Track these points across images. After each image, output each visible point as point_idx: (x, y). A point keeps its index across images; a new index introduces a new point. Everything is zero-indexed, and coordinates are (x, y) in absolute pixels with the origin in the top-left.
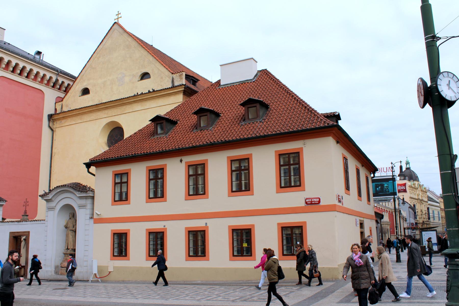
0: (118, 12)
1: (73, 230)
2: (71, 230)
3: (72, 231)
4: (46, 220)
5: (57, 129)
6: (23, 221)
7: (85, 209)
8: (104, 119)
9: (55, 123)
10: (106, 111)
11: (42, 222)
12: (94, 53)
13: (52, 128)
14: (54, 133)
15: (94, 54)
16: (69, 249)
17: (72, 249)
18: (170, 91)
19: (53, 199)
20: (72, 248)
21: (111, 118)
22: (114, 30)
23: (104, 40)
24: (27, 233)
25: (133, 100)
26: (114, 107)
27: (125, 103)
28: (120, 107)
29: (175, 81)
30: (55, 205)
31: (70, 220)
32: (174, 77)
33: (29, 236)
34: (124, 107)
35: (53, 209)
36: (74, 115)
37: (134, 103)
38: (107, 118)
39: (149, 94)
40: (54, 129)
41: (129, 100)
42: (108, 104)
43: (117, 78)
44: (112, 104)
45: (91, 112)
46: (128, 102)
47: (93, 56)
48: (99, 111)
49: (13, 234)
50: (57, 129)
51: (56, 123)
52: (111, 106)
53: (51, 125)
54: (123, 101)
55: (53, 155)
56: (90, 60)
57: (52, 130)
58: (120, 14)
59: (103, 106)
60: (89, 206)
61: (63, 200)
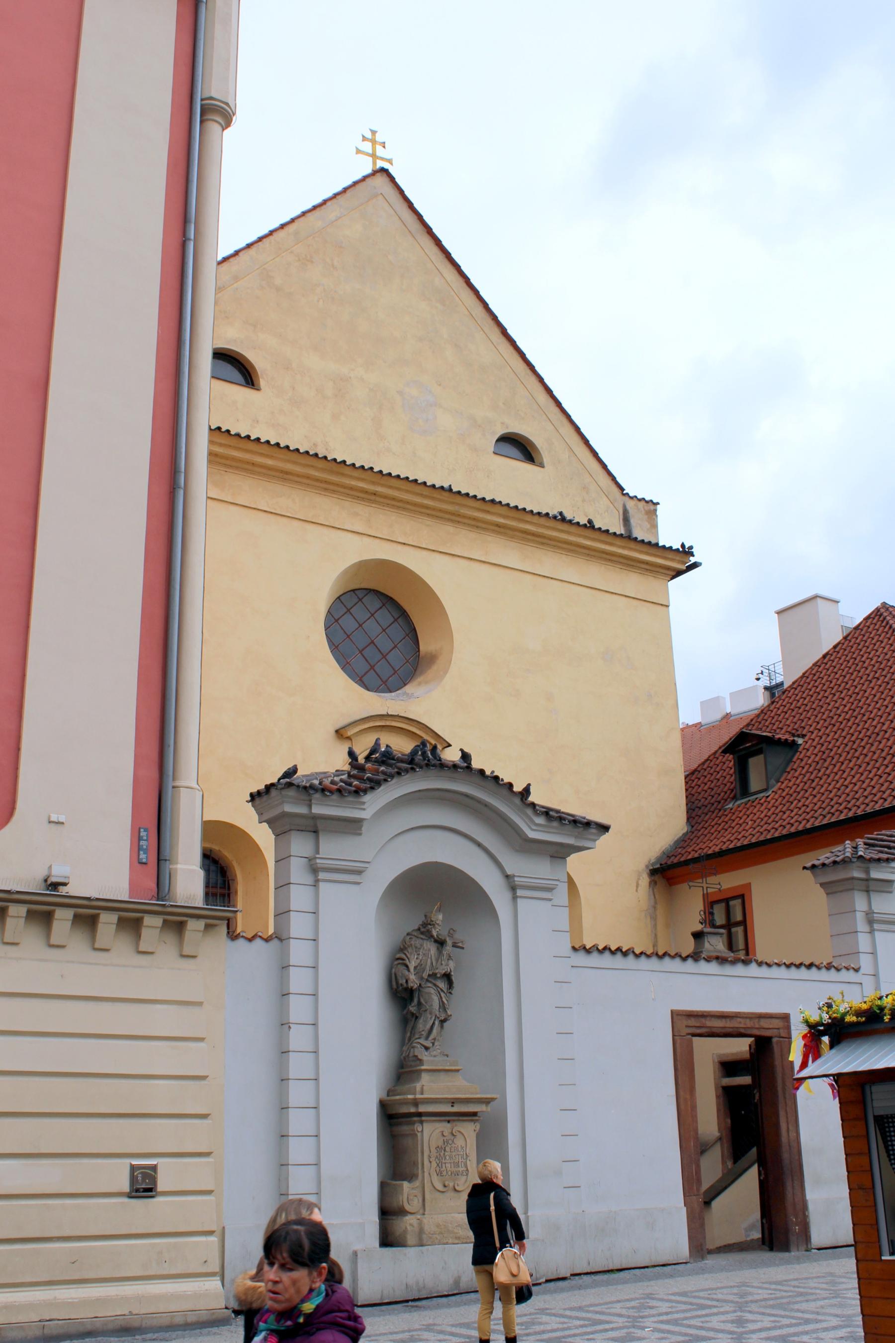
0: (374, 133)
8: (350, 535)
10: (363, 510)
12: (283, 226)
15: (281, 234)
18: (641, 552)
22: (375, 196)
23: (329, 204)
25: (501, 520)
26: (404, 509)
27: (464, 517)
28: (429, 521)
29: (633, 522)
32: (628, 507)
34: (450, 528)
37: (494, 531)
38: (366, 540)
39: (589, 533)
41: (488, 512)
42: (391, 487)
43: (400, 393)
44: (407, 491)
45: (284, 476)
46: (474, 519)
47: (275, 235)
48: (326, 489)
52: (394, 499)
54: (458, 504)
56: (260, 243)
58: (383, 145)
59: (362, 480)
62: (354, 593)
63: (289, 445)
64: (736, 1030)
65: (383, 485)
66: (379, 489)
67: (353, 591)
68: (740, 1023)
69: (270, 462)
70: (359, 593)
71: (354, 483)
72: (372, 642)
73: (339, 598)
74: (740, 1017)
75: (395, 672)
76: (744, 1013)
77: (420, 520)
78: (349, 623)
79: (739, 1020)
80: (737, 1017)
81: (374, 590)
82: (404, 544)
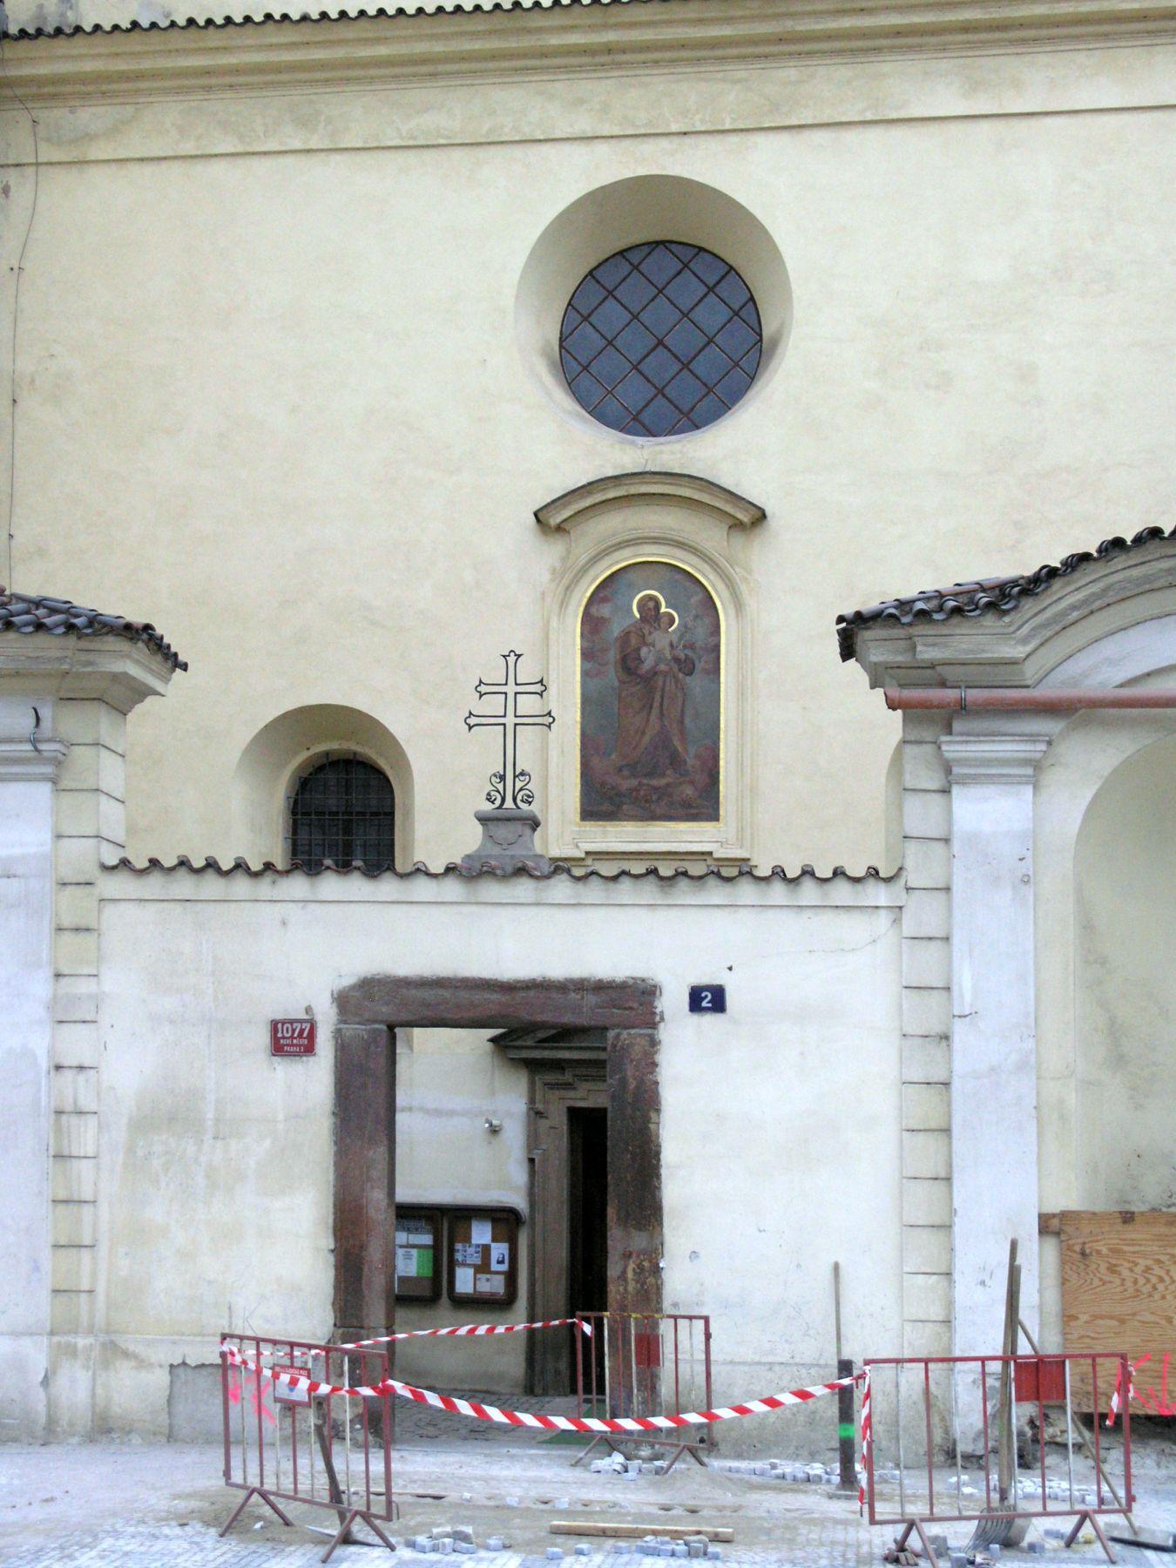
8: (566, 148)
21: (648, 147)
36: (236, 71)
38: (602, 149)
42: (632, 25)
62: (624, 257)
63: (402, 6)
65: (618, 26)
66: (611, 36)
67: (621, 253)
69: (382, 51)
70: (635, 257)
71: (555, 40)
72: (660, 343)
73: (591, 273)
75: (710, 390)
77: (720, 75)
78: (612, 319)
81: (663, 243)
82: (685, 134)
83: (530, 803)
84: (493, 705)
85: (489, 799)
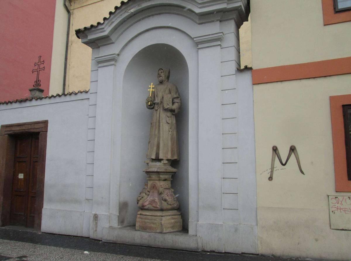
1: (172, 111)
2: (166, 110)
3: (169, 114)
4: (90, 92)
5: (75, 11)
6: (31, 100)
7: (219, 47)
9: (72, 4)
11: (80, 96)
13: (69, 9)
14: (72, 16)
16: (162, 160)
17: (167, 160)
19: (113, 38)
20: (169, 157)
24: (42, 125)
30: (117, 52)
31: (162, 87)
33: (47, 132)
35: (113, 63)
40: (71, 11)
49: (8, 129)
50: (75, 11)
51: (74, 3)
53: (67, 4)
55: (70, 44)
57: (68, 11)
60: (230, 39)
61: (147, 35)
64: (24, 131)
68: (26, 127)
74: (26, 125)
76: (28, 123)
79: (26, 126)
80: (25, 125)
83: (40, 86)
84: (37, 67)
85: (34, 86)
